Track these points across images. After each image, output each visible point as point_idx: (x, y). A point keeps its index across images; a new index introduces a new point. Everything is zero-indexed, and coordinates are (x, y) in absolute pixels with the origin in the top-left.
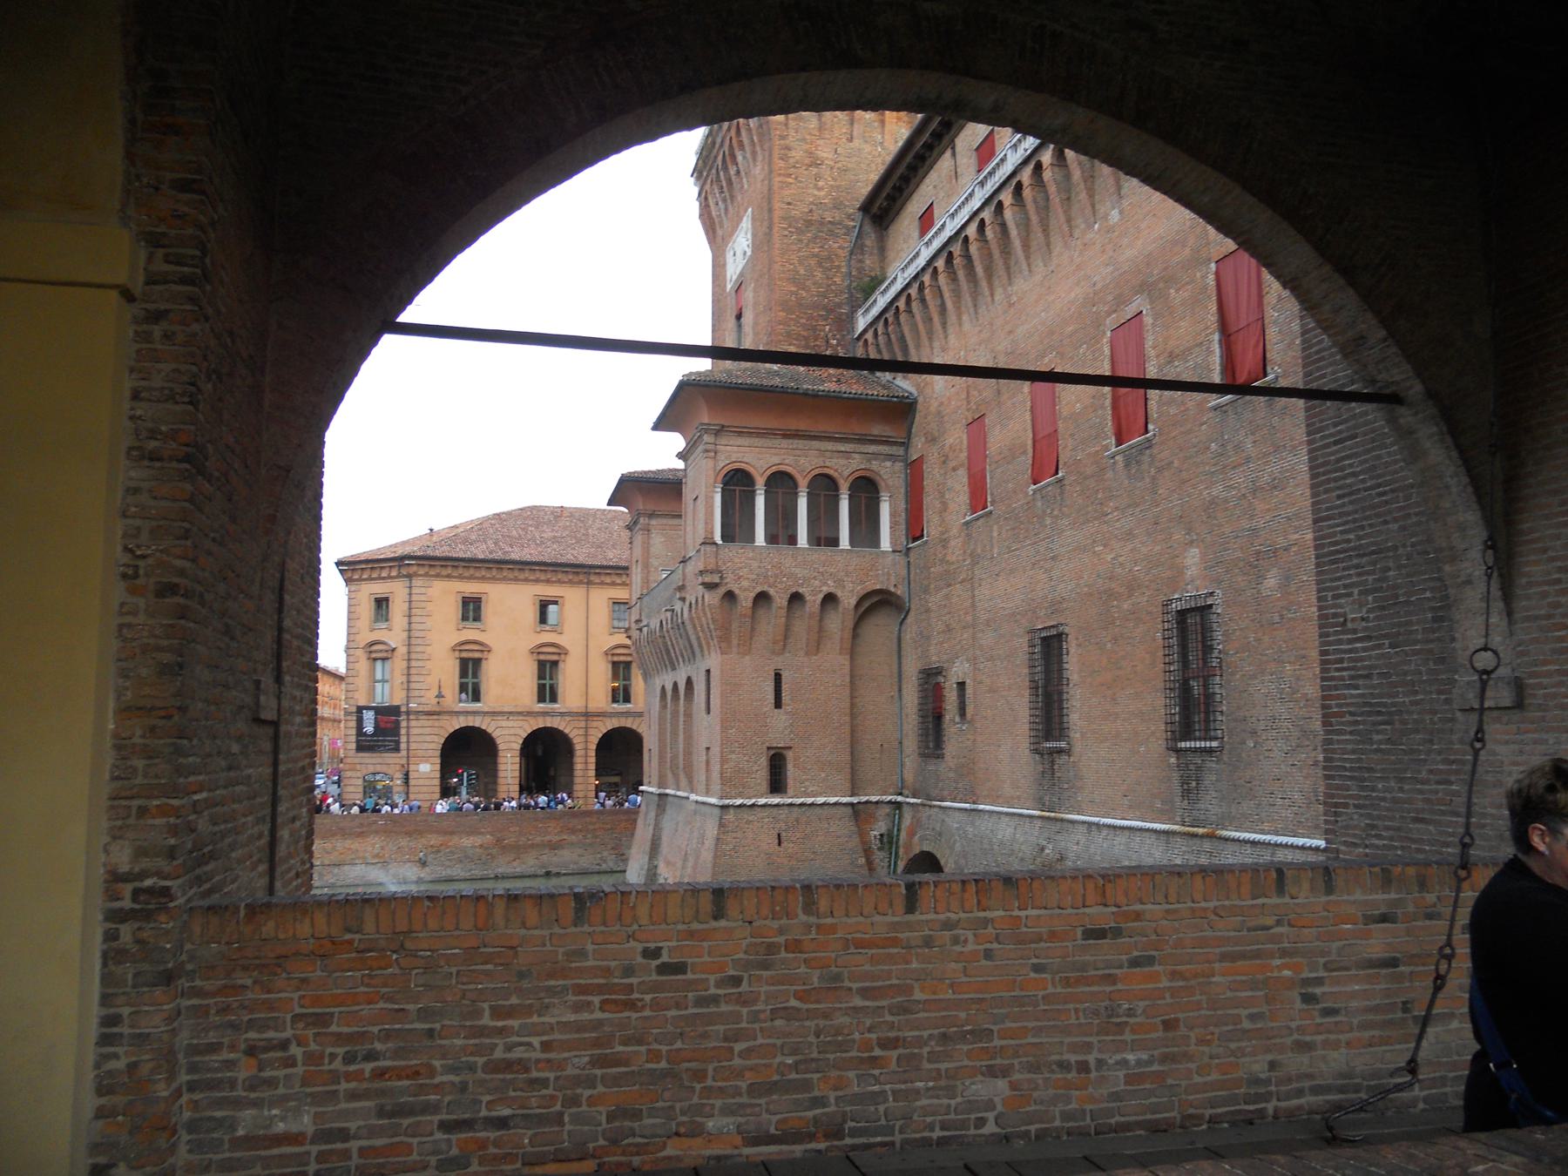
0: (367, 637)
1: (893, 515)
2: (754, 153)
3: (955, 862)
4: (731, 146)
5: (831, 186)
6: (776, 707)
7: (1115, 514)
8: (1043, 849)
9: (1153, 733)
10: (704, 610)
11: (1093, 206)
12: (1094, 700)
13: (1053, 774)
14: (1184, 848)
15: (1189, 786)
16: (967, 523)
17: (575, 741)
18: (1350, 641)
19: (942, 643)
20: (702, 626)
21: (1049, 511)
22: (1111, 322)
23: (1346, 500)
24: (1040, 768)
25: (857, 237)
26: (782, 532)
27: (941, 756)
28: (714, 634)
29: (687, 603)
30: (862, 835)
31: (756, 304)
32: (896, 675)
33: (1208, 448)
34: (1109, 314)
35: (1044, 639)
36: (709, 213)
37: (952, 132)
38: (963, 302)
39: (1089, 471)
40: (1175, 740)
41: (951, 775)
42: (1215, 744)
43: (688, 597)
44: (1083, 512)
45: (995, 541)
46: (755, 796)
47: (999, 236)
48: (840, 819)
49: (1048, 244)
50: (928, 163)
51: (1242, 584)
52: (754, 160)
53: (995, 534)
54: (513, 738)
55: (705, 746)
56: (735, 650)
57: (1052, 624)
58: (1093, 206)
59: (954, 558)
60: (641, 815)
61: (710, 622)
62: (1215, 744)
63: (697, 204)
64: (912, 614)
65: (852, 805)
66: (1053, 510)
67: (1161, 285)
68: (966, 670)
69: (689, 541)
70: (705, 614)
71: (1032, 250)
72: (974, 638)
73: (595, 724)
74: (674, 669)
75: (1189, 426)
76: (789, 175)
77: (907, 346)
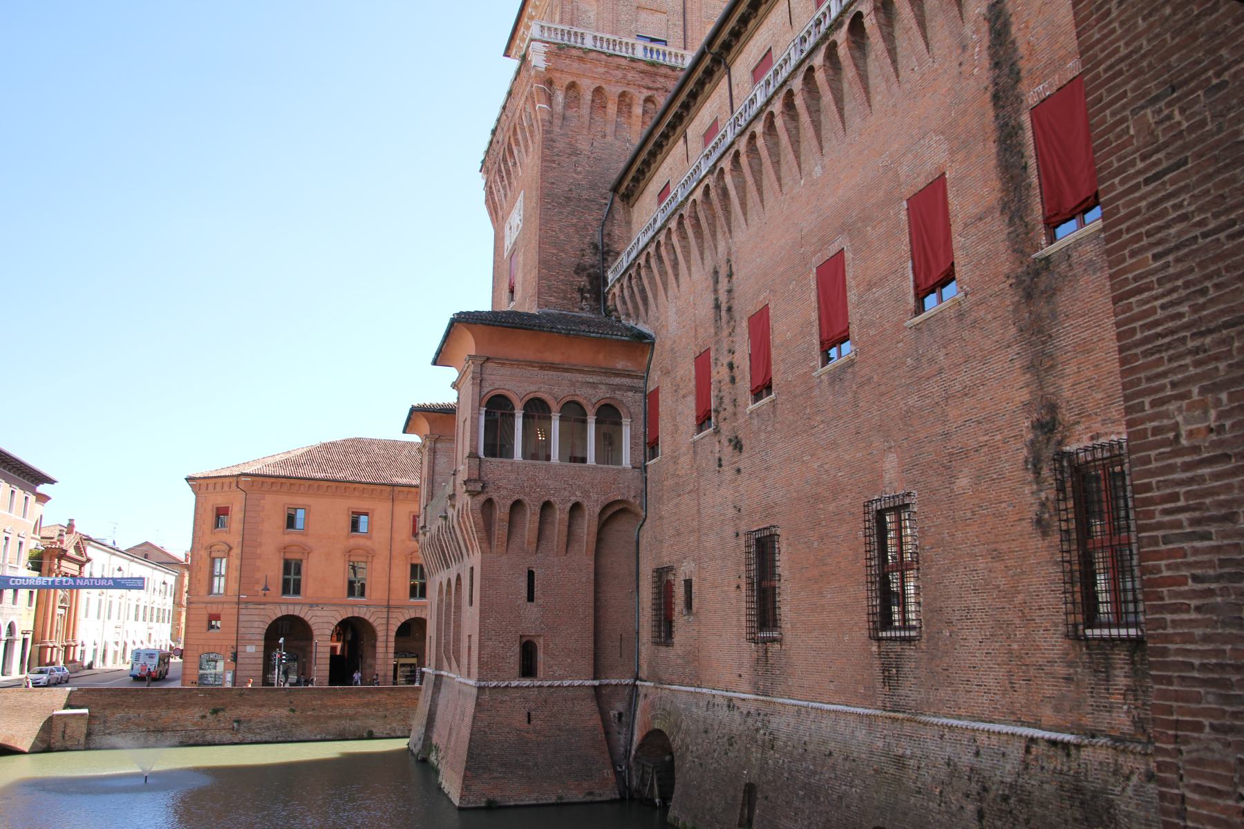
0: (209, 539)
2: (526, 147)
3: (682, 740)
4: (509, 144)
5: (588, 171)
6: (529, 600)
7: (821, 426)
10: (468, 515)
11: (799, 165)
12: (803, 593)
14: (885, 732)
15: (890, 673)
16: (695, 443)
17: (378, 629)
18: (1188, 467)
20: (467, 530)
21: (763, 427)
22: (817, 260)
23: (1170, 258)
24: (755, 655)
25: (608, 212)
26: (537, 452)
27: (672, 645)
28: (475, 535)
29: (456, 510)
30: (603, 713)
31: (525, 265)
32: (634, 575)
33: (904, 363)
34: (814, 253)
35: (758, 540)
36: (493, 199)
37: (684, 124)
38: (692, 256)
39: (798, 391)
40: (875, 629)
41: (680, 661)
42: (913, 633)
43: (457, 504)
44: (793, 427)
46: (508, 679)
47: (721, 198)
48: (583, 700)
49: (762, 201)
50: (665, 150)
51: (936, 484)
52: (526, 151)
54: (326, 625)
55: (468, 633)
56: (494, 550)
58: (799, 165)
60: (423, 692)
62: (913, 633)
63: (484, 193)
64: (648, 521)
65: (595, 687)
67: (860, 225)
69: (460, 457)
70: (468, 518)
71: (749, 207)
72: (699, 540)
73: (394, 615)
74: (448, 567)
75: (887, 345)
76: (554, 162)
77: (647, 296)
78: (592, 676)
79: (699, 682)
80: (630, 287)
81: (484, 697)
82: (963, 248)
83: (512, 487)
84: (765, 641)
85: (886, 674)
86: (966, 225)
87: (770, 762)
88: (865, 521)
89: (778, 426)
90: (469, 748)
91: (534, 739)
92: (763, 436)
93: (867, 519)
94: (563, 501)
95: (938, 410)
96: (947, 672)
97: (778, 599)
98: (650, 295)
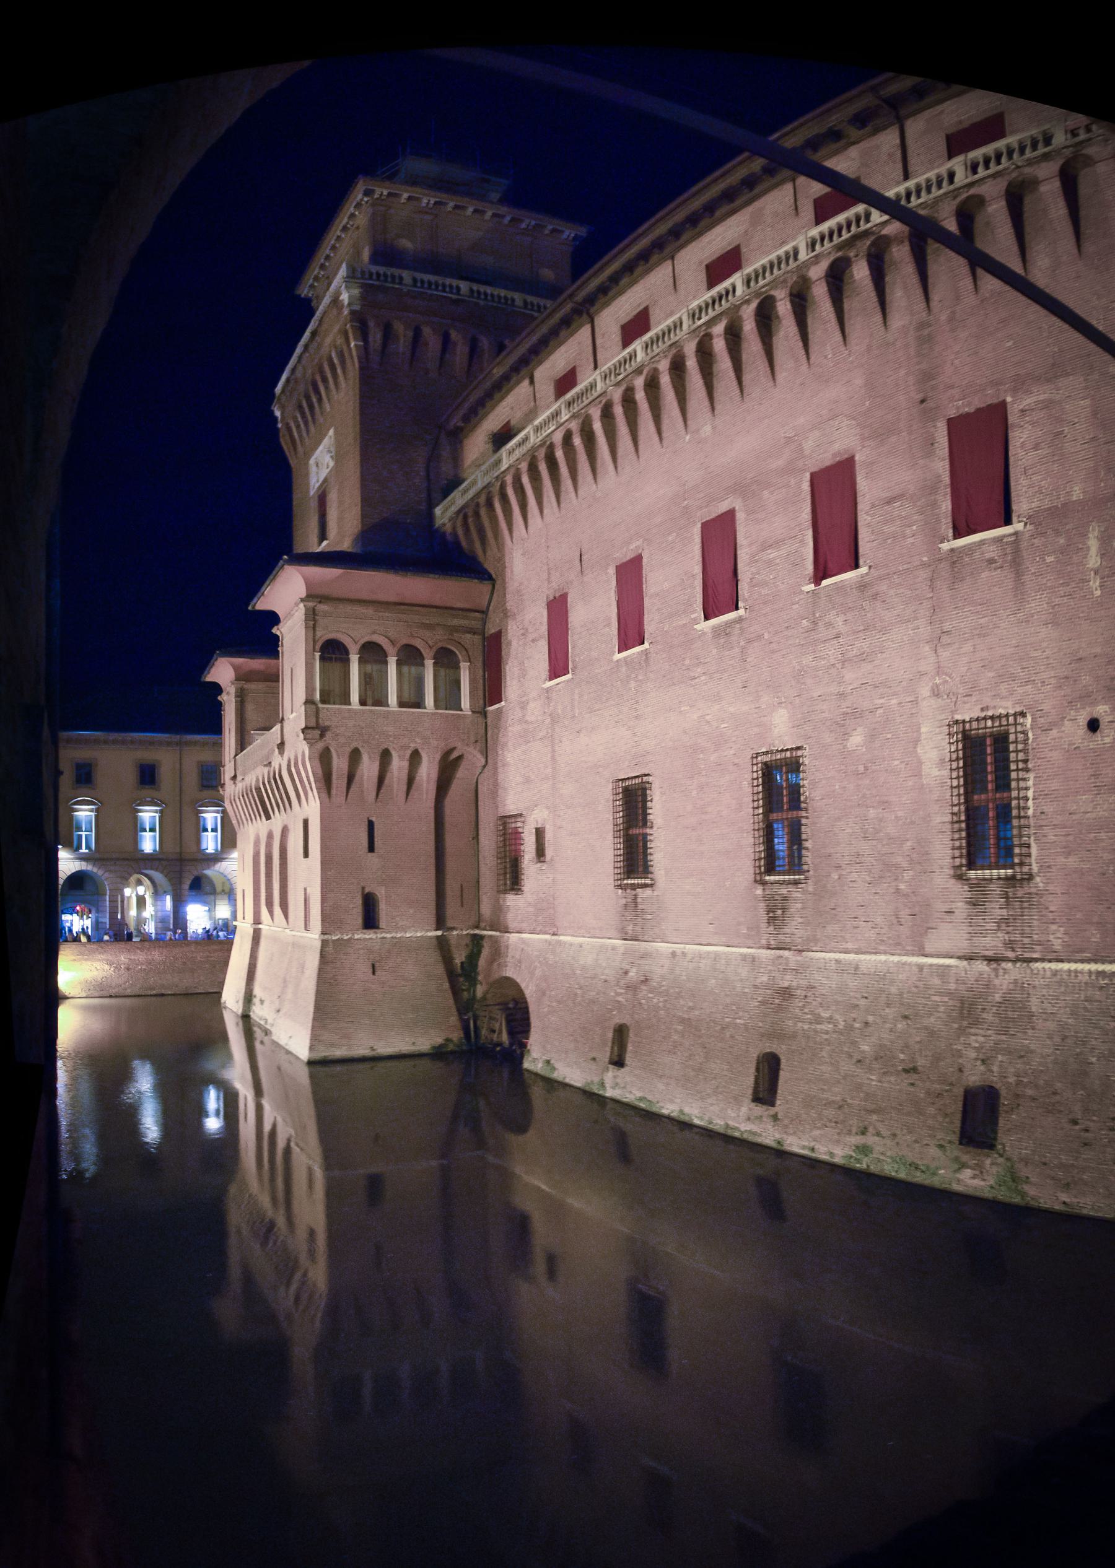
1: (473, 681)
8: (626, 973)
21: (633, 675)
24: (624, 901)
26: (373, 695)
35: (626, 790)
41: (531, 909)
53: (576, 697)
59: (533, 718)
68: (546, 817)
79: (555, 929)
80: (465, 524)
81: (327, 949)
82: (868, 525)
83: (350, 734)
84: (634, 887)
85: (771, 915)
86: (873, 506)
88: (753, 772)
89: (652, 676)
92: (633, 684)
93: (755, 769)
94: (404, 747)
95: (833, 671)
96: (833, 912)
97: (649, 846)
98: (489, 534)
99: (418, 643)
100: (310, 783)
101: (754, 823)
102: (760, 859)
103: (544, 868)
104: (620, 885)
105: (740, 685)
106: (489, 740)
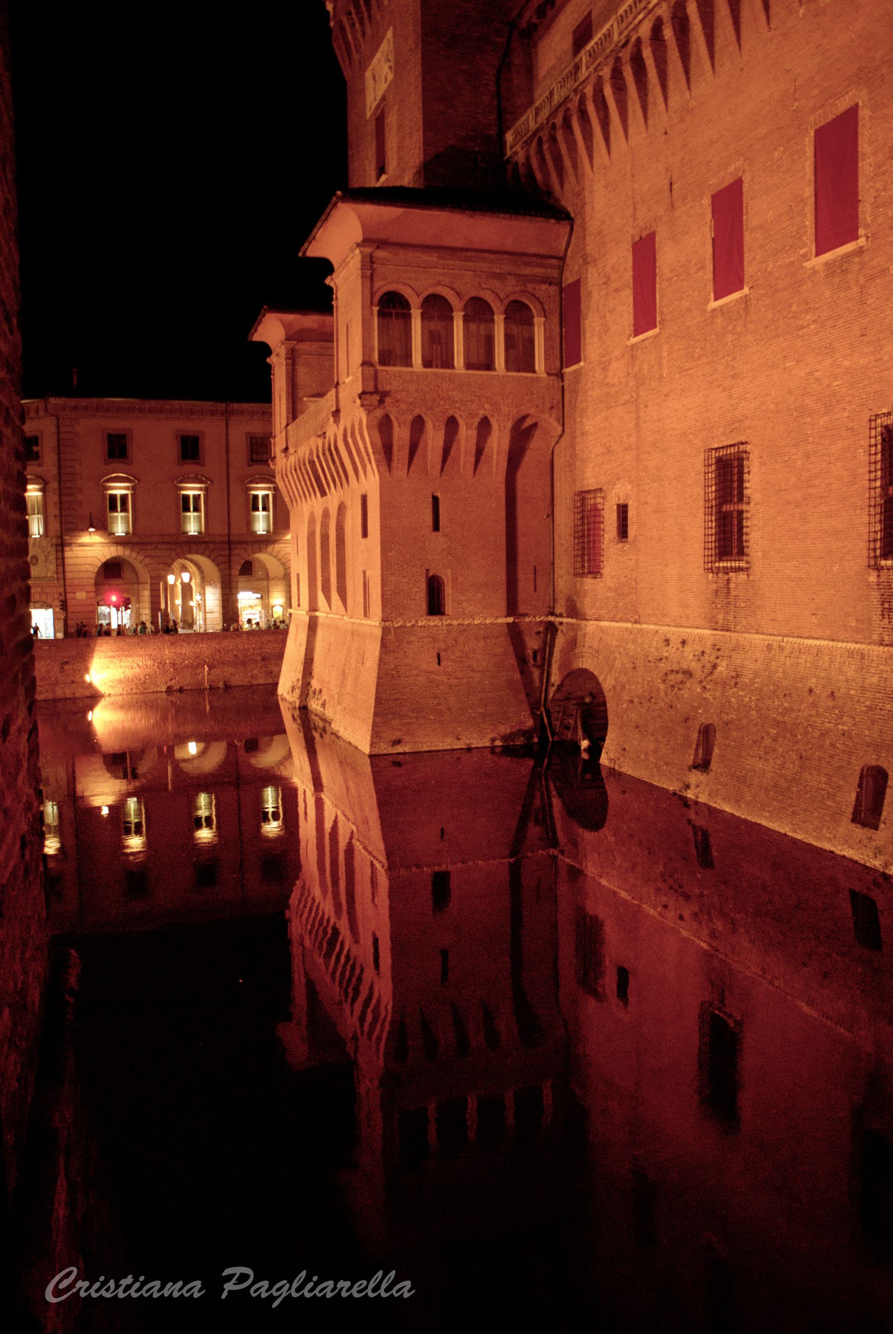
7: (812, 327)
9: (850, 551)
12: (779, 518)
13: (728, 592)
14: (882, 667)
19: (600, 465)
21: (730, 327)
24: (714, 587)
29: (341, 428)
32: (549, 499)
35: (719, 460)
44: (772, 327)
45: (664, 361)
53: (665, 354)
57: (732, 443)
59: (616, 380)
61: (369, 445)
66: (734, 327)
68: (628, 492)
78: (505, 613)
79: (637, 617)
80: (540, 151)
83: (411, 400)
84: (726, 571)
87: (733, 700)
88: (870, 437)
89: (751, 326)
90: (377, 693)
91: (446, 681)
92: (730, 337)
97: (745, 524)
98: (567, 163)
99: (488, 296)
100: (368, 455)
101: (869, 498)
102: (875, 540)
103: (625, 549)
104: (711, 569)
105: (858, 333)
106: (565, 406)
